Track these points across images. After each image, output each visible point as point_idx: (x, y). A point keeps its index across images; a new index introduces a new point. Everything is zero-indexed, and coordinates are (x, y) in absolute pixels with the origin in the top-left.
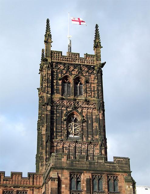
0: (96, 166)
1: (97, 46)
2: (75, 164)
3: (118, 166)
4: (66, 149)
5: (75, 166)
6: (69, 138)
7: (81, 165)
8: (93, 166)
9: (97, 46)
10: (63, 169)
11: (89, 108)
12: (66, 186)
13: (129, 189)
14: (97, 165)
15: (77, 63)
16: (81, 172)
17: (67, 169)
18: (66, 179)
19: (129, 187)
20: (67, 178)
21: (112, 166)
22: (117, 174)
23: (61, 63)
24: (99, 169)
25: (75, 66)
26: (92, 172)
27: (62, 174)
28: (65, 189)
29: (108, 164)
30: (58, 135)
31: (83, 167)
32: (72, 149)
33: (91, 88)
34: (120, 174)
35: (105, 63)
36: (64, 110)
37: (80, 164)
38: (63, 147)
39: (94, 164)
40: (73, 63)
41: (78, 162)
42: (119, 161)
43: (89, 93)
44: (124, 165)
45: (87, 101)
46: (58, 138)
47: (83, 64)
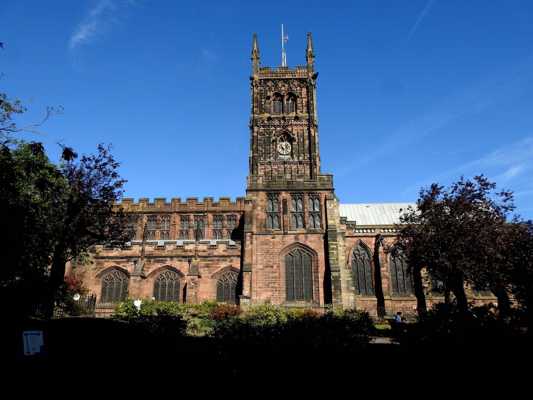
0: (294, 185)
2: (272, 184)
3: (319, 184)
4: (276, 171)
5: (272, 187)
7: (279, 186)
8: (291, 185)
10: (257, 190)
11: (301, 125)
12: (262, 209)
14: (296, 184)
15: (287, 77)
16: (278, 192)
18: (262, 200)
20: (263, 199)
21: (312, 184)
23: (268, 80)
25: (286, 81)
26: (291, 192)
28: (261, 211)
29: (309, 182)
30: (267, 156)
32: (282, 170)
33: (302, 103)
34: (321, 192)
35: (318, 73)
36: (274, 130)
37: (277, 185)
39: (293, 184)
40: (284, 77)
41: (275, 183)
42: (321, 178)
43: (301, 109)
45: (297, 118)
46: (267, 159)
47: (294, 77)
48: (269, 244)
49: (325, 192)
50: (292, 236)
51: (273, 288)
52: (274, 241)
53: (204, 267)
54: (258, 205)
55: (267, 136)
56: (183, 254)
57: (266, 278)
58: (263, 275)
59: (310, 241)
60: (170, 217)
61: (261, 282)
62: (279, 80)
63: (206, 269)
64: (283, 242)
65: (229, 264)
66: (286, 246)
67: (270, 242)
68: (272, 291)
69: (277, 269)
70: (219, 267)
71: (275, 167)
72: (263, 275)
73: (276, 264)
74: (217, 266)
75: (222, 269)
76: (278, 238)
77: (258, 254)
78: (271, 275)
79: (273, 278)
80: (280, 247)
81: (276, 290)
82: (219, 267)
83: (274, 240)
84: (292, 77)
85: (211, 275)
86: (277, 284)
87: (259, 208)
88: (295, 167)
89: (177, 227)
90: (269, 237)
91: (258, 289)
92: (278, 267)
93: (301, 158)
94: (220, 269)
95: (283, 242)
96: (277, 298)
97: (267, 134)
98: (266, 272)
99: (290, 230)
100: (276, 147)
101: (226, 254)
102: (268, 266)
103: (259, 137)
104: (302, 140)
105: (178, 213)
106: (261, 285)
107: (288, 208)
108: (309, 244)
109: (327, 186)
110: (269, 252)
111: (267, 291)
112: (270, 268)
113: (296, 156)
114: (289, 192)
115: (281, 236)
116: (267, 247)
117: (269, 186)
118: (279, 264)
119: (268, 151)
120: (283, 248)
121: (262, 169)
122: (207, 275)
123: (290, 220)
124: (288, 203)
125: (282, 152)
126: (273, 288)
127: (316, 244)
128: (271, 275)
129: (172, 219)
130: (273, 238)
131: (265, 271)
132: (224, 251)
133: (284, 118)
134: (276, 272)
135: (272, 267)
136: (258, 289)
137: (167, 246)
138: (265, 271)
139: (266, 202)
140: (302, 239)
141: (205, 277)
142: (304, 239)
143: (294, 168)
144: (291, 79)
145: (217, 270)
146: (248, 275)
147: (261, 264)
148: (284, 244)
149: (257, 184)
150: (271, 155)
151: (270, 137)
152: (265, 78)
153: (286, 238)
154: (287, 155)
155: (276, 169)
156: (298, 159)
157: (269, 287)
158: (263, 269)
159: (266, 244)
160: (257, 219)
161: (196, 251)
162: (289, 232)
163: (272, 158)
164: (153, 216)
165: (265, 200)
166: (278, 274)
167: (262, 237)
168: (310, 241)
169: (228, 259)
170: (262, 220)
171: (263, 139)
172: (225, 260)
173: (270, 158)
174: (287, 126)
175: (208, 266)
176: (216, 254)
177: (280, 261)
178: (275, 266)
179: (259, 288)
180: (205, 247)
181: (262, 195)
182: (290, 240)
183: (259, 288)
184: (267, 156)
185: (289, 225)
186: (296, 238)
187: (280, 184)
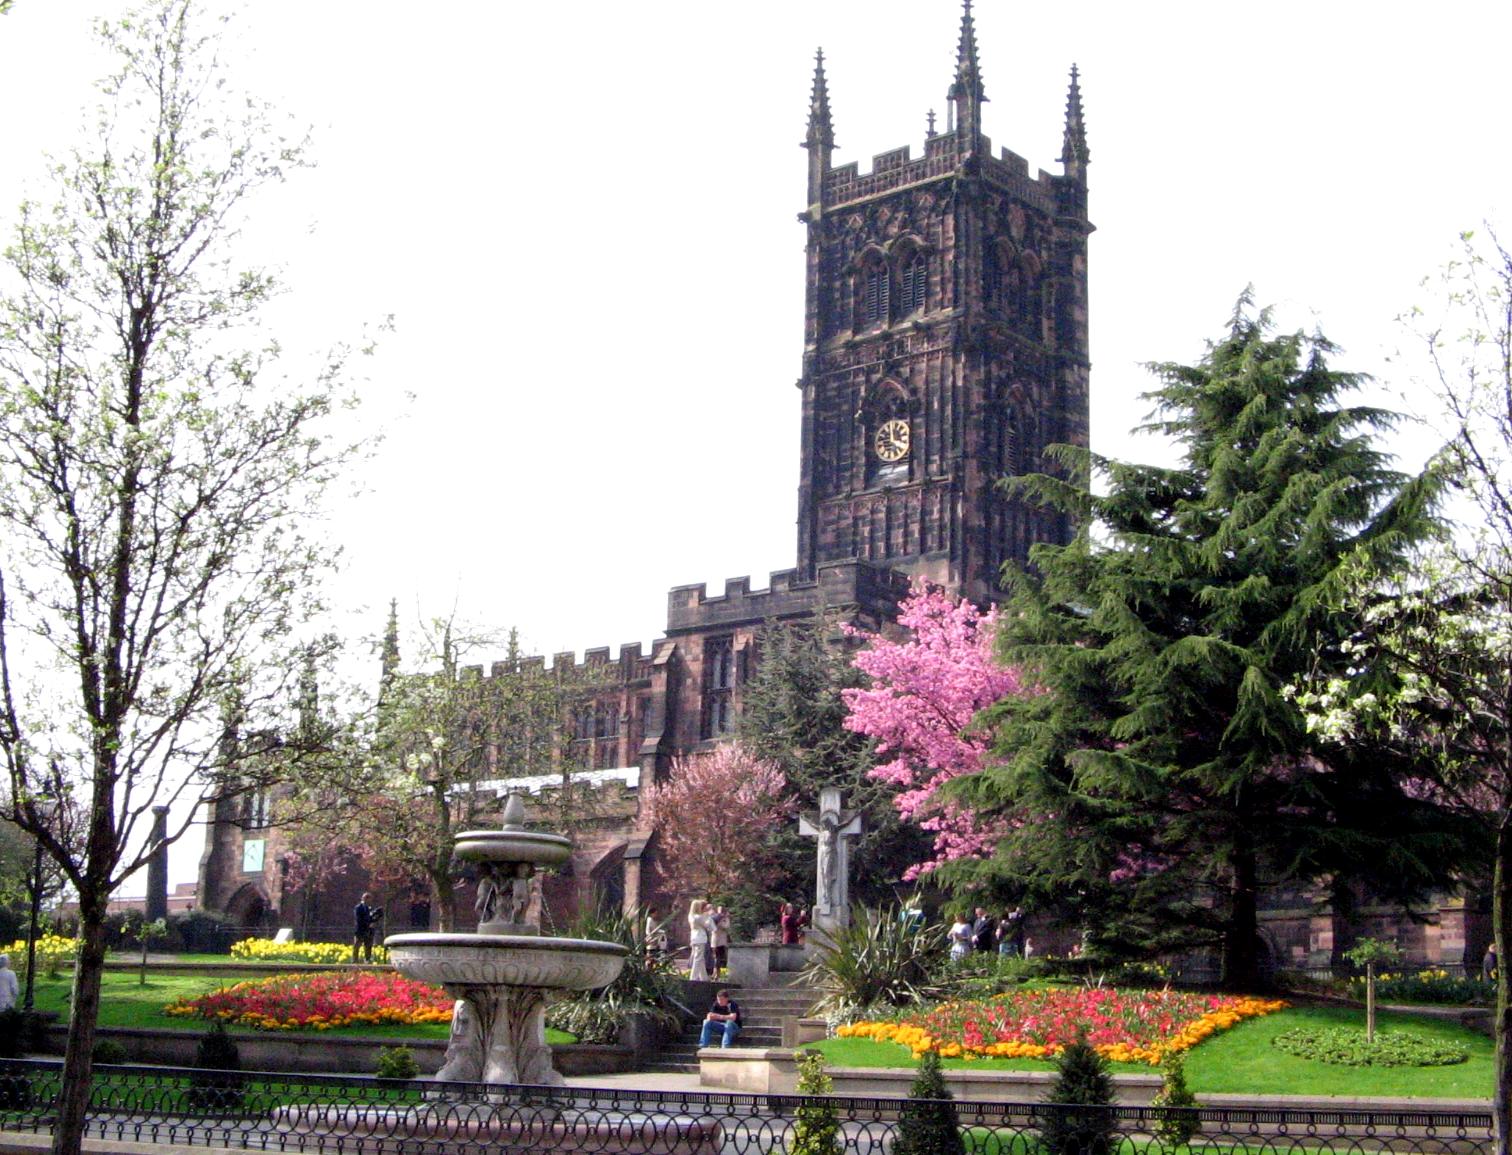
1: (968, 89)
2: (721, 609)
9: (968, 89)
15: (901, 188)
17: (698, 630)
18: (695, 659)
23: (850, 210)
44: (840, 587)
47: (920, 182)
62: (882, 201)
70: (605, 847)
75: (611, 854)
82: (605, 847)
84: (914, 184)
93: (934, 468)
94: (607, 852)
100: (870, 443)
104: (936, 405)
117: (711, 617)
121: (831, 523)
133: (886, 336)
144: (908, 192)
145: (603, 856)
149: (687, 613)
152: (839, 206)
154: (899, 462)
156: (927, 472)
174: (899, 364)
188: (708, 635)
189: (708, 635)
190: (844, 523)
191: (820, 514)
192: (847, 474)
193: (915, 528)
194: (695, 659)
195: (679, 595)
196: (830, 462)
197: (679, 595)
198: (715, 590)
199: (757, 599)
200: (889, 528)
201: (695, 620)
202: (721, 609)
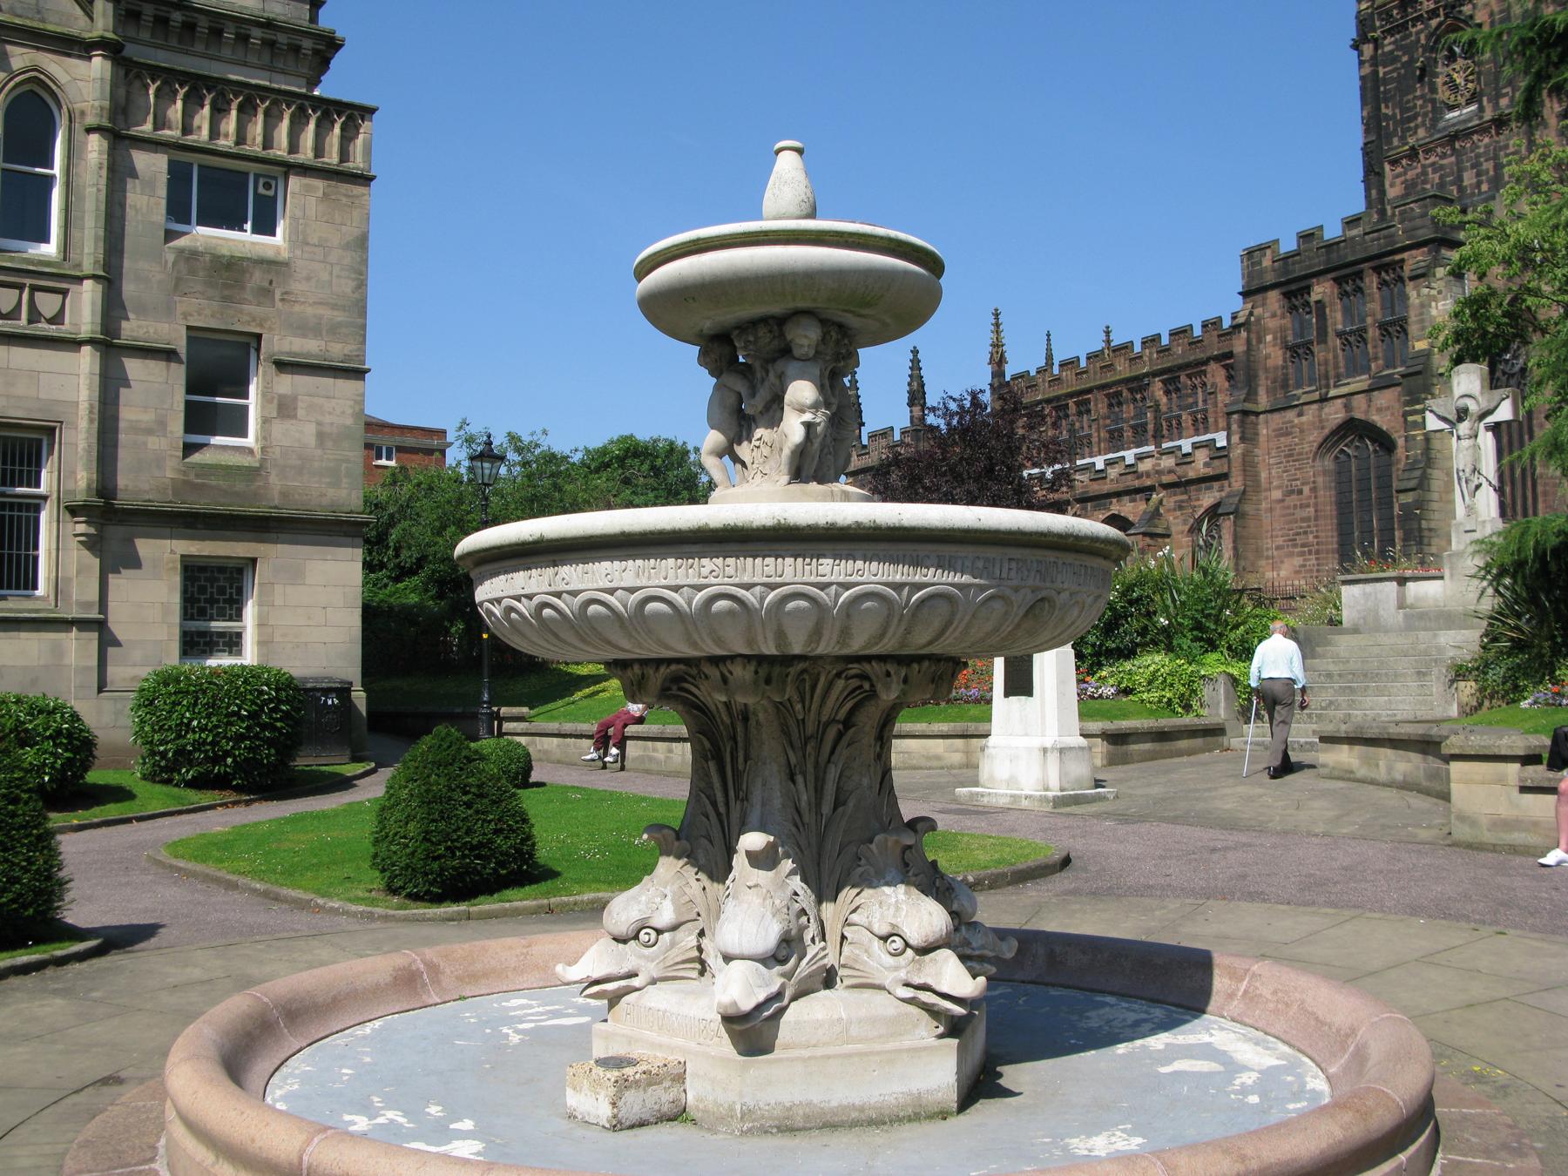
0: (1342, 253)
4: (1434, 172)
6: (1441, 125)
10: (1264, 289)
12: (1275, 338)
13: (1417, 301)
14: (1346, 248)
18: (1274, 316)
19: (1419, 295)
22: (1397, 257)
24: (1351, 258)
26: (1333, 275)
27: (1264, 305)
30: (1409, 129)
31: (1310, 267)
34: (1405, 255)
36: (1421, 31)
38: (1424, 167)
41: (1297, 258)
44: (1418, 222)
48: (1291, 433)
49: (1414, 252)
50: (1339, 401)
51: (1303, 546)
52: (1302, 424)
53: (1175, 510)
54: (1266, 331)
55: (1405, 59)
56: (1137, 484)
57: (1290, 522)
58: (1284, 516)
59: (1379, 410)
60: (1204, 373)
61: (1280, 533)
63: (1178, 513)
64: (1321, 421)
65: (1217, 495)
66: (1327, 431)
67: (1292, 427)
68: (1302, 554)
69: (1310, 497)
70: (1201, 506)
71: (1433, 159)
72: (1284, 516)
73: (1307, 483)
74: (1196, 503)
76: (1311, 412)
77: (1272, 461)
78: (1300, 513)
79: (1303, 520)
80: (1315, 437)
81: (1310, 552)
82: (1201, 506)
83: (1304, 419)
85: (1187, 528)
86: (1311, 537)
87: (1269, 338)
88: (1487, 140)
89: (1220, 397)
90: (1291, 415)
91: (1275, 553)
92: (1314, 490)
95: (1321, 421)
96: (1311, 571)
97: (1404, 54)
98: (1288, 508)
99: (1336, 386)
101: (1209, 471)
102: (1292, 492)
103: (1381, 71)
105: (1217, 359)
106: (1280, 541)
107: (1329, 322)
108: (1376, 418)
109: (1420, 232)
110: (1292, 455)
111: (1291, 555)
112: (1294, 497)
113: (1489, 101)
114: (1330, 276)
115: (1315, 406)
116: (1288, 440)
117: (1287, 272)
118: (1314, 482)
119: (1409, 109)
120: (1320, 440)
121: (1397, 176)
122: (1180, 528)
123: (1335, 357)
124: (1328, 310)
125: (1452, 97)
126: (1303, 546)
127: (1392, 414)
128: (1300, 513)
129: (1209, 380)
130: (1300, 415)
131: (1286, 504)
132: (1206, 465)
134: (1308, 506)
135: (1300, 492)
136: (1275, 553)
137: (1109, 470)
138: (1286, 504)
139: (1283, 317)
140: (1360, 408)
141: (1178, 533)
142: (1364, 406)
143: (1486, 146)
146: (1228, 522)
147: (1278, 487)
148: (1323, 428)
149: (1262, 272)
150: (1420, 119)
151: (1412, 60)
153: (1326, 410)
154: (1468, 103)
155: (1433, 164)
156: (1496, 106)
157: (1295, 546)
158: (1283, 501)
159: (1287, 434)
160: (1266, 370)
161: (1158, 472)
162: (1332, 393)
163: (1421, 133)
164: (1171, 377)
165: (1279, 312)
166: (1312, 510)
167: (1276, 416)
168: (1379, 410)
169: (1216, 485)
170: (1276, 368)
171: (1395, 75)
172: (1210, 488)
173: (1416, 133)
175: (1181, 508)
176: (1192, 475)
177: (1318, 474)
178: (1306, 490)
179: (1278, 548)
180: (1168, 462)
181: (1274, 297)
182: (1335, 414)
183: (1278, 548)
184: (1409, 129)
185: (1332, 373)
186: (1347, 407)
187: (1310, 259)
188: (1284, 289)
189: (1284, 289)
190: (1411, 174)
191: (1387, 167)
192: (1412, 125)
193: (1488, 166)
194: (1274, 316)
195: (1252, 255)
196: (1394, 115)
197: (1252, 255)
198: (1289, 245)
199: (1331, 246)
200: (1460, 170)
201: (1270, 278)
202: (1293, 264)
